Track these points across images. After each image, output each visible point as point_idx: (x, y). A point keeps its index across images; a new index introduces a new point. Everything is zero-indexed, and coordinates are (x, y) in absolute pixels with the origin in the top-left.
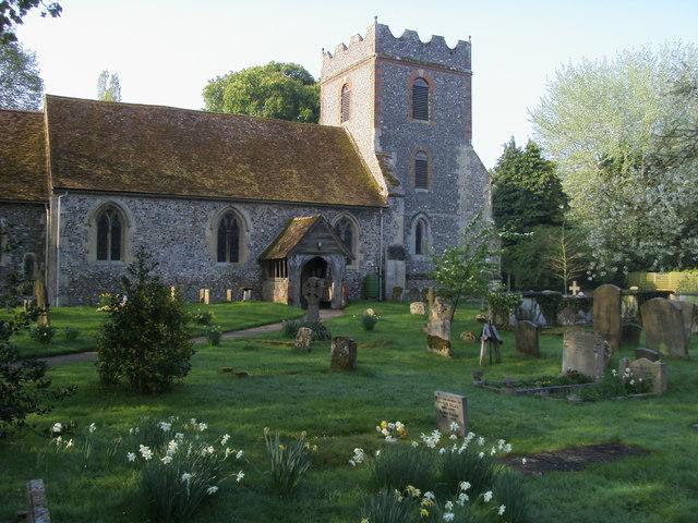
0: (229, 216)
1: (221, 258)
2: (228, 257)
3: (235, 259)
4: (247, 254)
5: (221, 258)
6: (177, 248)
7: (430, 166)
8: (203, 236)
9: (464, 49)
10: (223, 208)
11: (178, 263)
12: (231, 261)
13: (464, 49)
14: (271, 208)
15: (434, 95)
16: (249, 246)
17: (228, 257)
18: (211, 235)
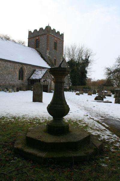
0: (21, 68)
1: (19, 79)
2: (21, 79)
3: (22, 79)
4: (25, 78)
5: (19, 79)
6: (10, 76)
7: (57, 60)
8: (16, 73)
9: (62, 35)
10: (21, 66)
11: (10, 80)
12: (22, 80)
13: (62, 35)
14: (30, 67)
15: (58, 45)
16: (26, 76)
17: (21, 79)
18: (18, 73)
